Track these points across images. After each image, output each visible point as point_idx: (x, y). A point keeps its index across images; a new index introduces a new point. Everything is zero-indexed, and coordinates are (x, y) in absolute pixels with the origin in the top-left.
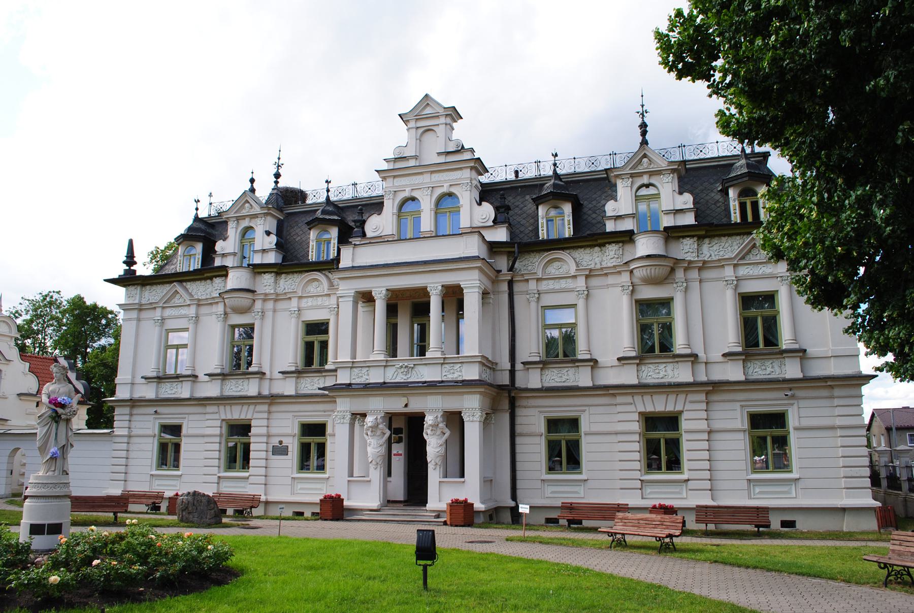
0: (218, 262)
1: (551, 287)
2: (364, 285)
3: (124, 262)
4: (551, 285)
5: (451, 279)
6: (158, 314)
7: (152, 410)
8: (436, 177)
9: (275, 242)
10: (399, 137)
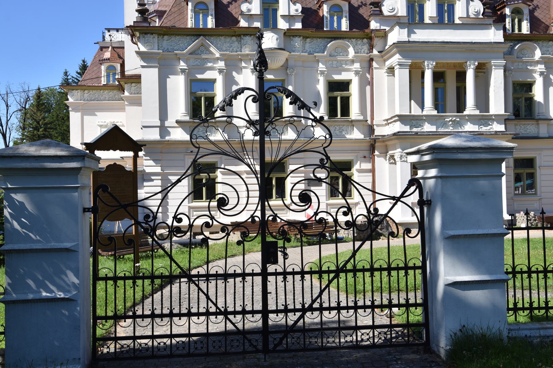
0: (243, 23)
1: (520, 67)
3: (137, 11)
6: (183, 65)
9: (300, 10)
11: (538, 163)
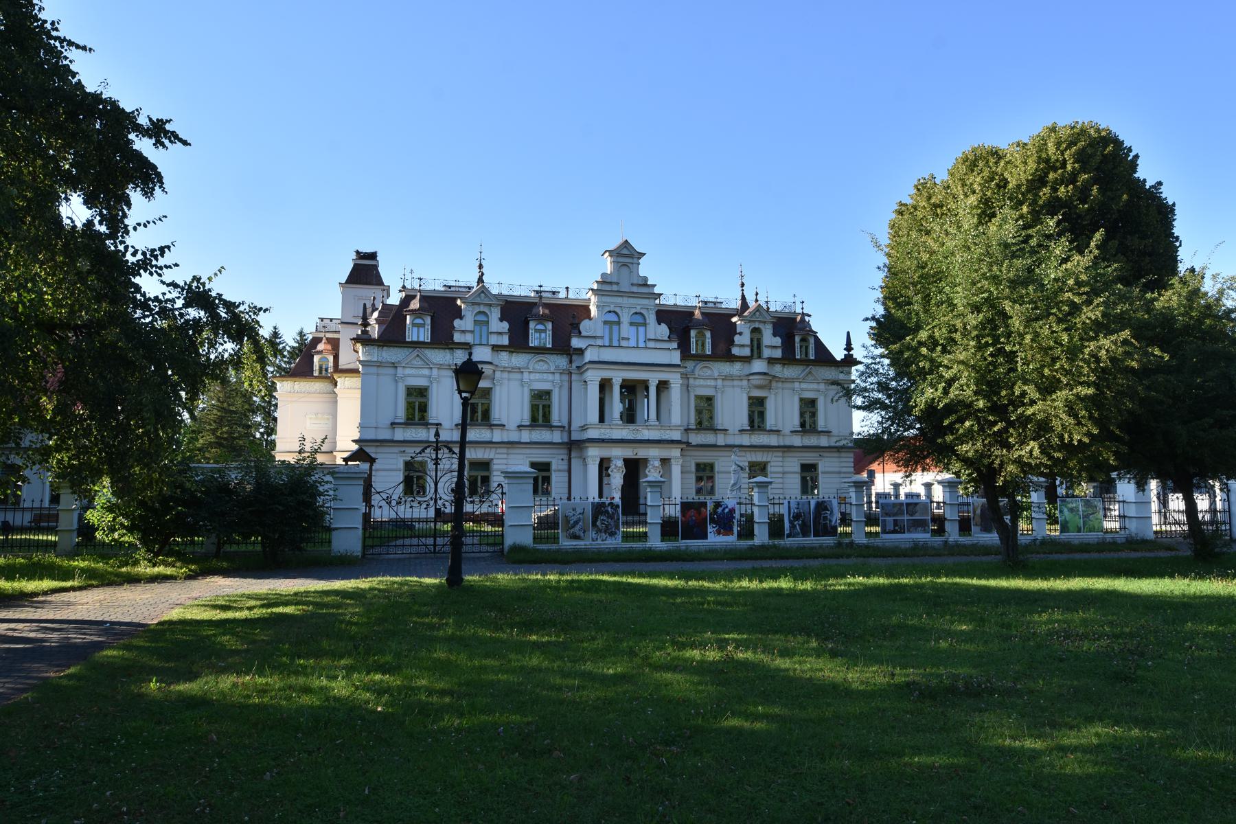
2: (607, 374)
4: (702, 382)
5: (664, 376)
7: (396, 450)
8: (632, 301)
10: (608, 266)
11: (716, 469)
